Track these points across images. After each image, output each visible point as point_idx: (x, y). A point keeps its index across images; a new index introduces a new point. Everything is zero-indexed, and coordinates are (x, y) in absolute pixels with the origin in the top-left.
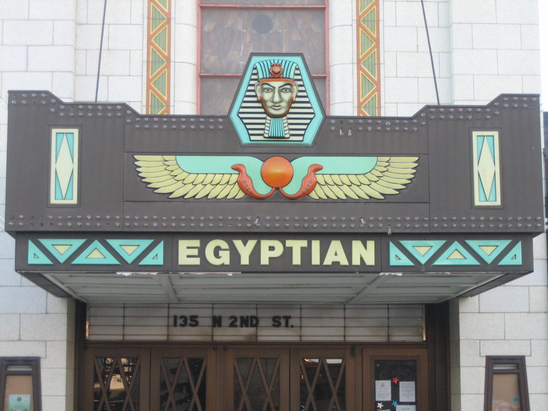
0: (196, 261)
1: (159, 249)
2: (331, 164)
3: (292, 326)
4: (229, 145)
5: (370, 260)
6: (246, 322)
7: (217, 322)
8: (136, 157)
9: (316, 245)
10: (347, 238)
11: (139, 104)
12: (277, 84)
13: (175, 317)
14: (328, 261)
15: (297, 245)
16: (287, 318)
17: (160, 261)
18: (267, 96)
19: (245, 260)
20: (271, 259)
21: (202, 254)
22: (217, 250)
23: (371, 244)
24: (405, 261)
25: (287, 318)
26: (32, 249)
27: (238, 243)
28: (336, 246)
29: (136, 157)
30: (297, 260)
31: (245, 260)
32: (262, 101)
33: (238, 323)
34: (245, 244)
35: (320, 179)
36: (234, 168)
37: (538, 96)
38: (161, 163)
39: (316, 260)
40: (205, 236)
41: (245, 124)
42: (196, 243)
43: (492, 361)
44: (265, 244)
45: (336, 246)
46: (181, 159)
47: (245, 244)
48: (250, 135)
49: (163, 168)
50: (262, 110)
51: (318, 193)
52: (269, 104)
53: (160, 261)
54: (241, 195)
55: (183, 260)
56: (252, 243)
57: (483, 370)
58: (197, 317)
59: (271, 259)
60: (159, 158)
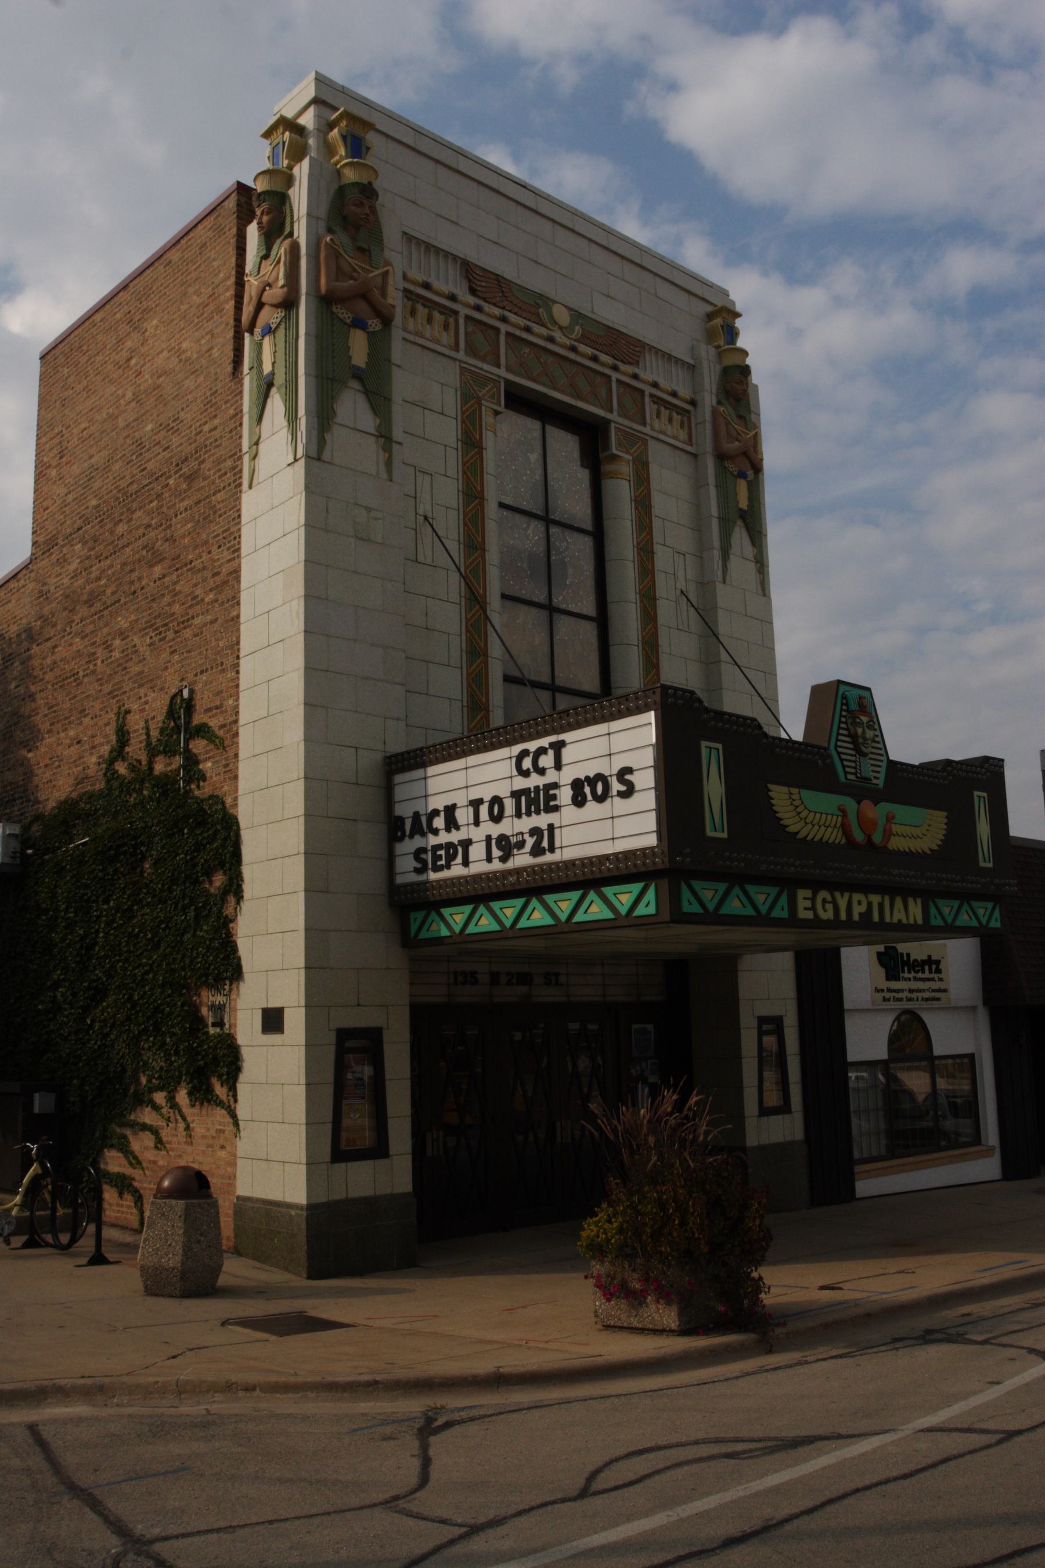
0: (809, 915)
1: (784, 900)
2: (904, 813)
3: (562, 985)
4: (829, 784)
5: (920, 921)
6: (524, 979)
7: (495, 978)
8: (770, 786)
9: (887, 899)
10: (906, 892)
11: (459, 704)
12: (865, 719)
13: (455, 973)
14: (895, 920)
15: (875, 899)
16: (557, 975)
17: (785, 914)
18: (860, 731)
19: (843, 916)
20: (860, 914)
21: (813, 908)
22: (824, 901)
23: (919, 901)
24: (939, 922)
25: (557, 975)
26: (686, 894)
27: (837, 895)
28: (899, 902)
29: (770, 786)
30: (876, 918)
31: (843, 916)
32: (854, 738)
33: (514, 981)
34: (842, 895)
35: (895, 828)
36: (840, 809)
37: (1003, 760)
38: (787, 796)
39: (888, 919)
40: (816, 885)
41: (842, 760)
42: (808, 893)
43: (762, 1020)
44: (857, 897)
45: (899, 902)
46: (804, 793)
47: (842, 895)
48: (846, 773)
49: (789, 802)
50: (851, 746)
51: (895, 843)
52: (861, 740)
53: (785, 914)
54: (844, 841)
55: (804, 914)
56: (846, 895)
57: (755, 1031)
58: (476, 973)
59: (860, 914)
60: (785, 789)
